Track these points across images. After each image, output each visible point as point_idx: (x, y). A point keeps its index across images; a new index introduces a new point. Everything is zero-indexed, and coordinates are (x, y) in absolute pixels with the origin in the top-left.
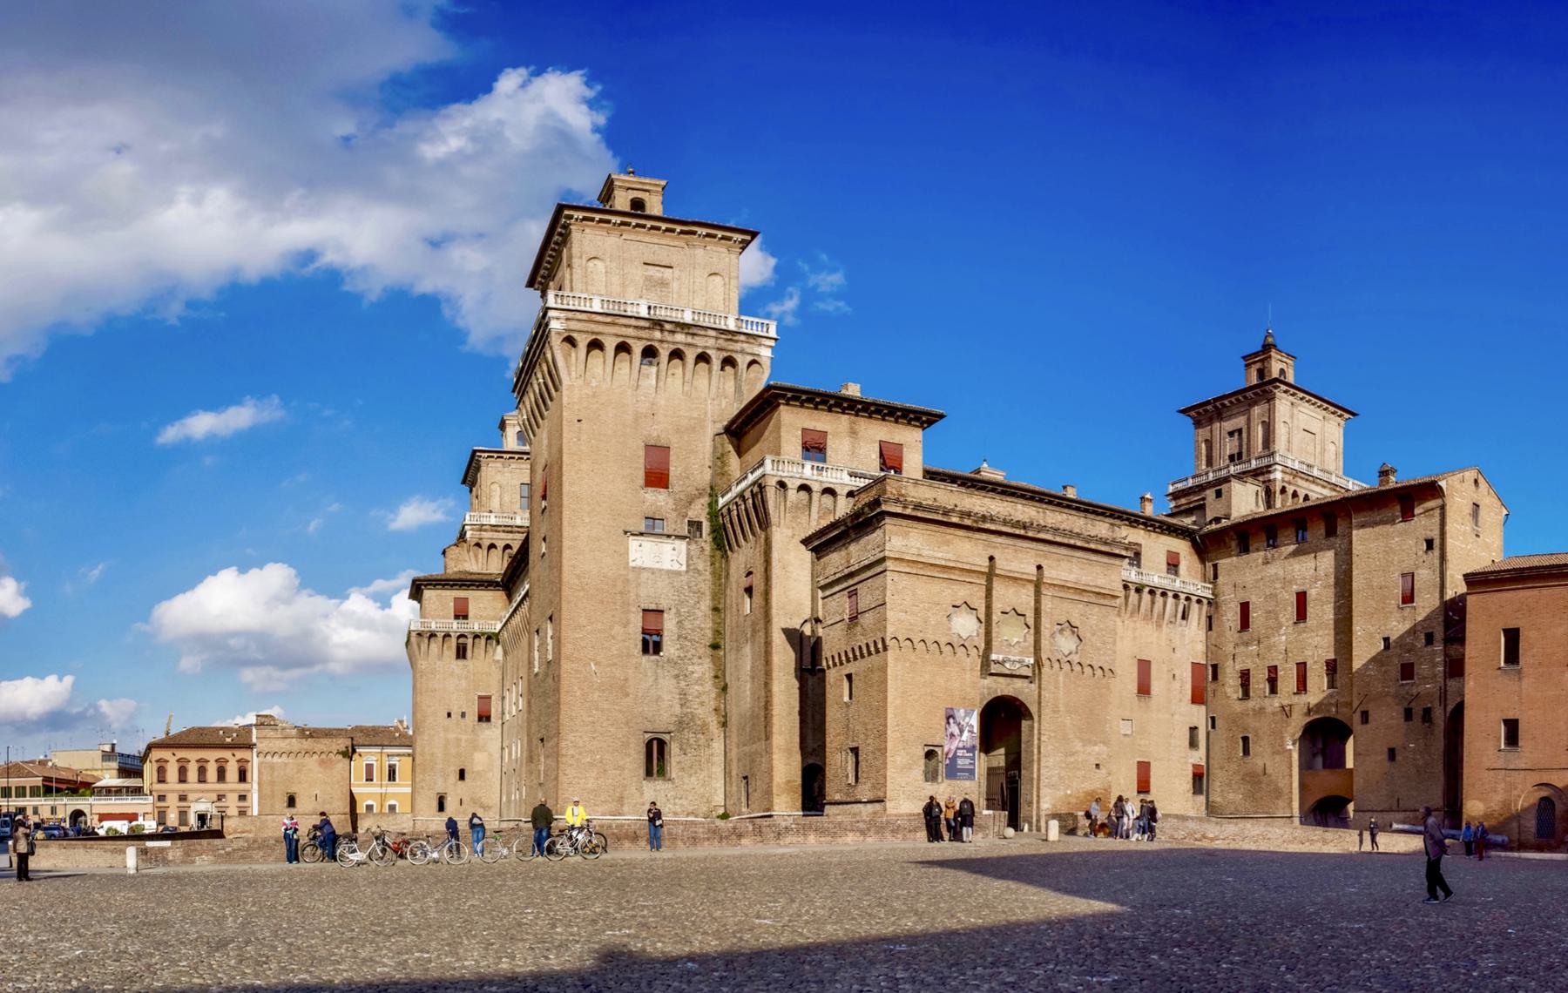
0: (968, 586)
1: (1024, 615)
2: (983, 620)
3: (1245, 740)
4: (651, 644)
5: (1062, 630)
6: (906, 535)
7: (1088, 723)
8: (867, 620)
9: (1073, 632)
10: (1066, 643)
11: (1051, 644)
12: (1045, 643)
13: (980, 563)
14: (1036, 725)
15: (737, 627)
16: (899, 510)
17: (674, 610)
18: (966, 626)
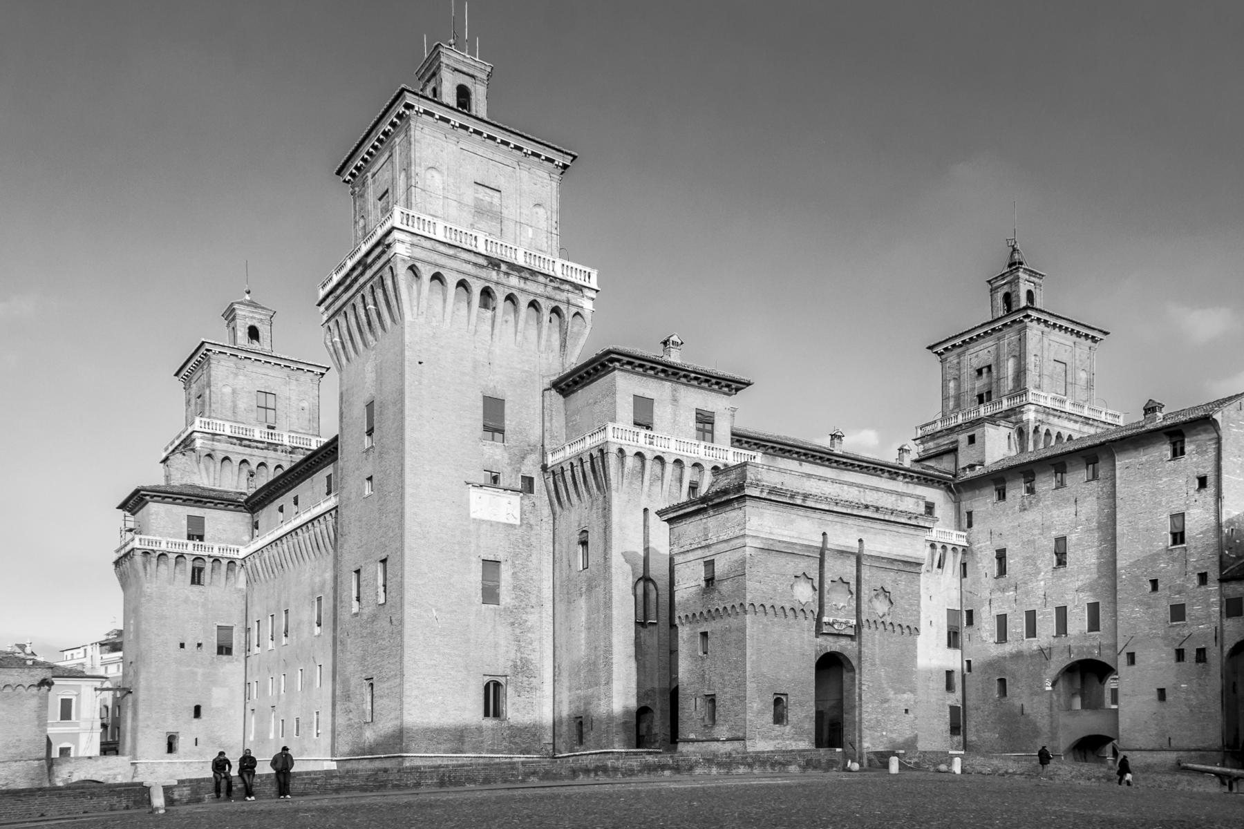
0: (807, 559)
1: (848, 583)
2: (817, 588)
3: (1002, 682)
4: (490, 594)
5: (877, 594)
6: (761, 515)
7: (899, 674)
8: (725, 587)
9: (886, 596)
10: (881, 607)
11: (869, 608)
12: (864, 607)
13: (816, 539)
14: (857, 676)
15: (569, 580)
16: (756, 493)
17: (510, 562)
18: (804, 593)
